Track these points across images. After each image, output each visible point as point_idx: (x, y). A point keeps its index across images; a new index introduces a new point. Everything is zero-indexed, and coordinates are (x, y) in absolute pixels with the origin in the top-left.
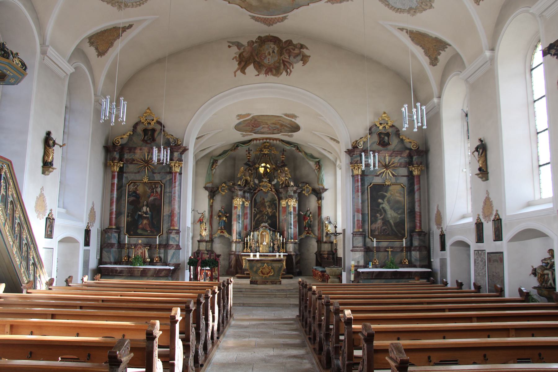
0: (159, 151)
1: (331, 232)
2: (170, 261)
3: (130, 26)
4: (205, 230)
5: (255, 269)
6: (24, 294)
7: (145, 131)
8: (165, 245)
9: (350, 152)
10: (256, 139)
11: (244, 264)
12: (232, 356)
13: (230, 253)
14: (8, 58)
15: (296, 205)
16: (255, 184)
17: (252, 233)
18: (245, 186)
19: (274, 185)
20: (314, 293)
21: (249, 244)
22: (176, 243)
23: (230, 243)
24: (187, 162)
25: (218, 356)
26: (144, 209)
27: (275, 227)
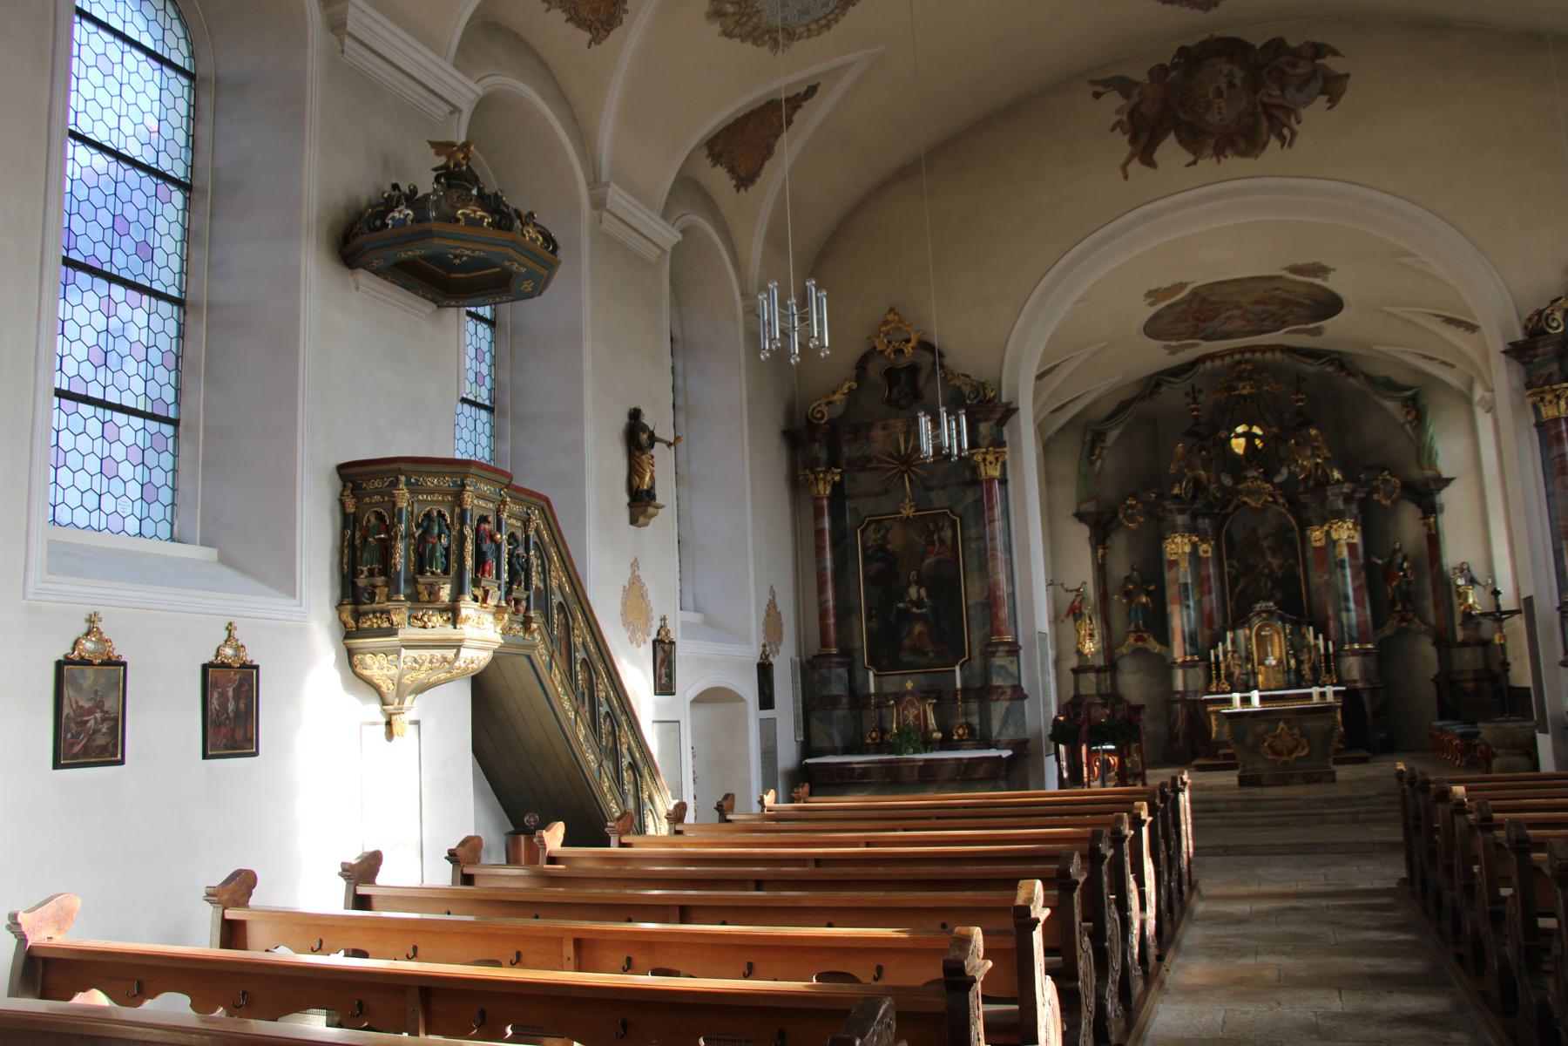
0: (936, 424)
1: (1478, 609)
2: (1000, 733)
3: (811, 91)
4: (1091, 635)
5: (1249, 740)
6: (614, 848)
7: (891, 374)
8: (981, 688)
9: (1516, 352)
10: (1211, 357)
11: (1214, 729)
12: (1207, 1016)
13: (1169, 697)
14: (509, 229)
15: (1357, 539)
16: (1222, 487)
17: (1229, 635)
18: (1194, 497)
19: (1282, 486)
20: (1460, 807)
21: (1223, 666)
22: (1009, 682)
23: (1164, 668)
24: (1017, 448)
25: (1166, 1015)
26: (913, 592)
27: (1299, 609)
